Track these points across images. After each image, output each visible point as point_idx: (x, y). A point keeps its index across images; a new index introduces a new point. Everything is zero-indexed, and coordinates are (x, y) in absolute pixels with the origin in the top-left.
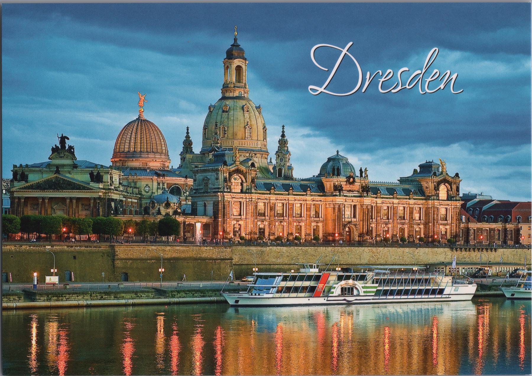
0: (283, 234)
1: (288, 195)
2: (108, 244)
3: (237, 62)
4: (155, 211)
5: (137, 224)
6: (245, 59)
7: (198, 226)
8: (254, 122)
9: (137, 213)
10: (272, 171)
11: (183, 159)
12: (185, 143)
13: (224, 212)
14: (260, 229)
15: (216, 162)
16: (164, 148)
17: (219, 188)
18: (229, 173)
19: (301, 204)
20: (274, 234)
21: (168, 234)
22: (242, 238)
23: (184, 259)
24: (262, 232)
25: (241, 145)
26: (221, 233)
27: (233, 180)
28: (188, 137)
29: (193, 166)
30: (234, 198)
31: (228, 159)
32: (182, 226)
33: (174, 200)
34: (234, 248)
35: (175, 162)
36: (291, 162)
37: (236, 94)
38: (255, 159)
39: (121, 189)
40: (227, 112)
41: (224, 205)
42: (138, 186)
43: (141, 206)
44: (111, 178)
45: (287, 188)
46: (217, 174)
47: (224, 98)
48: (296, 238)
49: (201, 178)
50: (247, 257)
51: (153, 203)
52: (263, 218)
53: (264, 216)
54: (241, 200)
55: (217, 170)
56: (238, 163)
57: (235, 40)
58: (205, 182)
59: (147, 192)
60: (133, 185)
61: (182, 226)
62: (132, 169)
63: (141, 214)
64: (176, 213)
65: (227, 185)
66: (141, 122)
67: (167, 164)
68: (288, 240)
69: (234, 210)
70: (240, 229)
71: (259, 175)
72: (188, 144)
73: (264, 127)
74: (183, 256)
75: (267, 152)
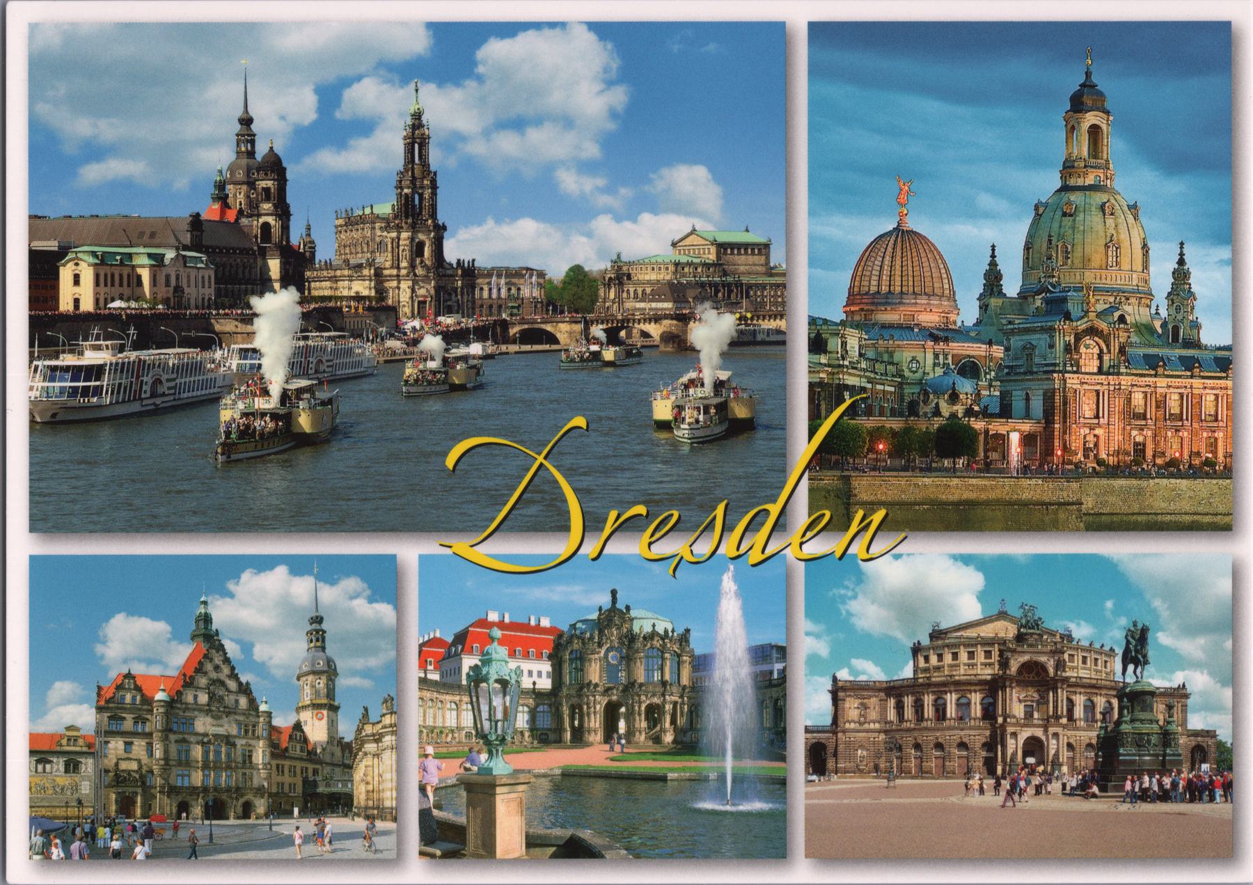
0: (1181, 455)
1: (1192, 377)
2: (838, 473)
3: (1091, 118)
4: (928, 409)
5: (894, 434)
6: (1108, 113)
7: (1015, 438)
8: (1124, 236)
9: (893, 413)
10: (1160, 331)
11: (984, 308)
12: (987, 275)
13: (1065, 411)
14: (1136, 444)
15: (1048, 313)
16: (946, 286)
17: (1055, 365)
18: (1076, 335)
19: (1217, 396)
20: (1163, 453)
21: (954, 455)
22: (1100, 462)
23: (987, 503)
24: (1140, 449)
25: (1098, 281)
26: (1059, 453)
27: (1082, 350)
28: (993, 264)
29: (1004, 322)
30: (1084, 384)
31: (1074, 308)
32: (982, 438)
33: (966, 387)
34: (1085, 481)
35: (968, 314)
36: (1197, 313)
37: (1090, 180)
38: (1127, 308)
39: (863, 366)
40: (1071, 215)
41: (1065, 398)
42: (896, 360)
43: (902, 398)
44: (844, 344)
45: (1189, 365)
46: (1052, 337)
47: (1065, 188)
48: (1208, 463)
49: (1020, 344)
50: (1112, 499)
51: (926, 394)
52: (1143, 422)
53: (1145, 418)
54: (1098, 387)
55: (1050, 330)
56: (1092, 315)
57: (1088, 74)
58: (1027, 352)
59: (914, 372)
60: (886, 357)
61: (982, 438)
62: (884, 326)
63: (901, 414)
64: (969, 412)
65: (1071, 359)
66: (903, 237)
67: (952, 317)
68: (1191, 466)
69: (1086, 407)
70: (1096, 445)
71: (1134, 339)
72: (993, 278)
73: (1145, 247)
74: (983, 497)
75: (1150, 294)
